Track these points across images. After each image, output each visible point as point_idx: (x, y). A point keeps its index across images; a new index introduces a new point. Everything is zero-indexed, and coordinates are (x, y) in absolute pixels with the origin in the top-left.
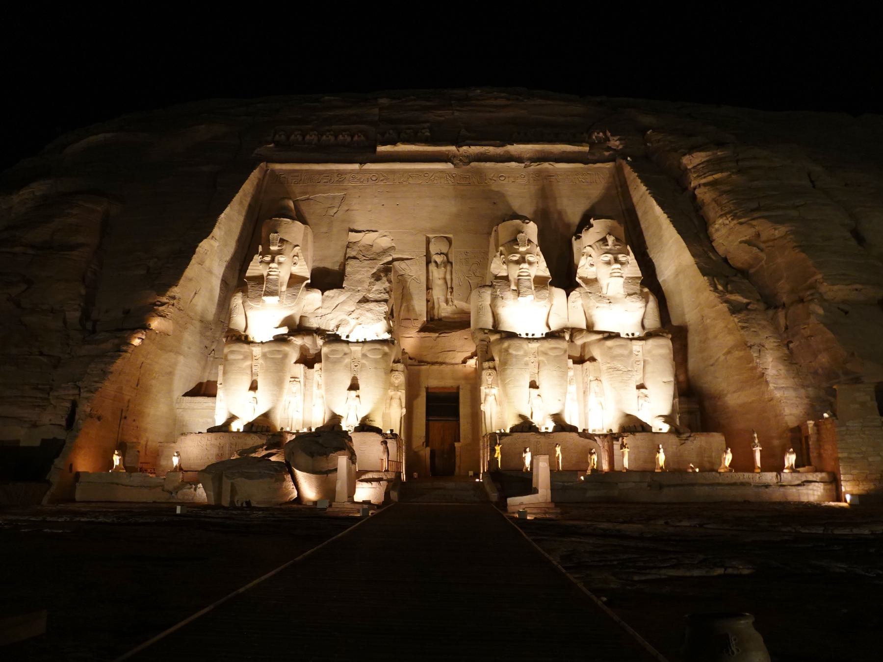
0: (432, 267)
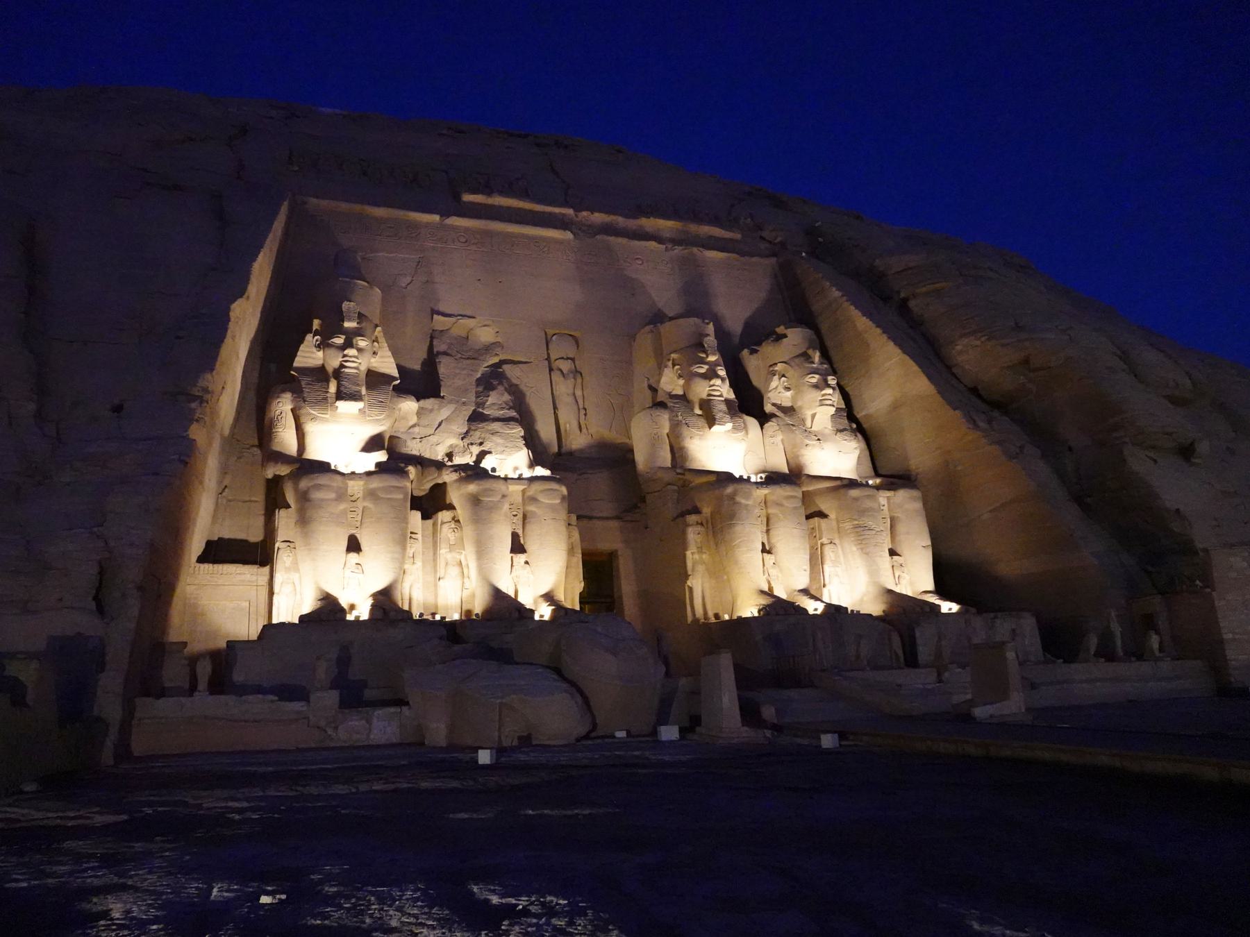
0: (556, 377)
